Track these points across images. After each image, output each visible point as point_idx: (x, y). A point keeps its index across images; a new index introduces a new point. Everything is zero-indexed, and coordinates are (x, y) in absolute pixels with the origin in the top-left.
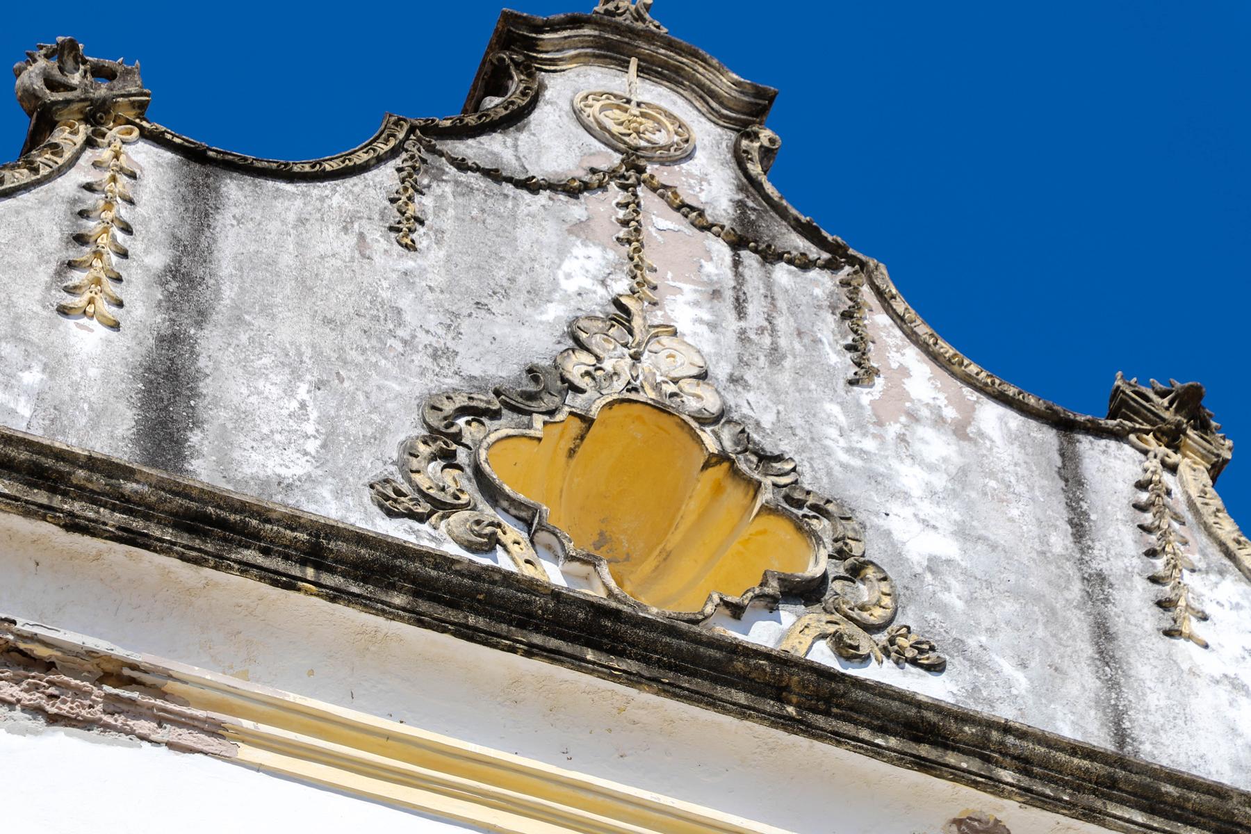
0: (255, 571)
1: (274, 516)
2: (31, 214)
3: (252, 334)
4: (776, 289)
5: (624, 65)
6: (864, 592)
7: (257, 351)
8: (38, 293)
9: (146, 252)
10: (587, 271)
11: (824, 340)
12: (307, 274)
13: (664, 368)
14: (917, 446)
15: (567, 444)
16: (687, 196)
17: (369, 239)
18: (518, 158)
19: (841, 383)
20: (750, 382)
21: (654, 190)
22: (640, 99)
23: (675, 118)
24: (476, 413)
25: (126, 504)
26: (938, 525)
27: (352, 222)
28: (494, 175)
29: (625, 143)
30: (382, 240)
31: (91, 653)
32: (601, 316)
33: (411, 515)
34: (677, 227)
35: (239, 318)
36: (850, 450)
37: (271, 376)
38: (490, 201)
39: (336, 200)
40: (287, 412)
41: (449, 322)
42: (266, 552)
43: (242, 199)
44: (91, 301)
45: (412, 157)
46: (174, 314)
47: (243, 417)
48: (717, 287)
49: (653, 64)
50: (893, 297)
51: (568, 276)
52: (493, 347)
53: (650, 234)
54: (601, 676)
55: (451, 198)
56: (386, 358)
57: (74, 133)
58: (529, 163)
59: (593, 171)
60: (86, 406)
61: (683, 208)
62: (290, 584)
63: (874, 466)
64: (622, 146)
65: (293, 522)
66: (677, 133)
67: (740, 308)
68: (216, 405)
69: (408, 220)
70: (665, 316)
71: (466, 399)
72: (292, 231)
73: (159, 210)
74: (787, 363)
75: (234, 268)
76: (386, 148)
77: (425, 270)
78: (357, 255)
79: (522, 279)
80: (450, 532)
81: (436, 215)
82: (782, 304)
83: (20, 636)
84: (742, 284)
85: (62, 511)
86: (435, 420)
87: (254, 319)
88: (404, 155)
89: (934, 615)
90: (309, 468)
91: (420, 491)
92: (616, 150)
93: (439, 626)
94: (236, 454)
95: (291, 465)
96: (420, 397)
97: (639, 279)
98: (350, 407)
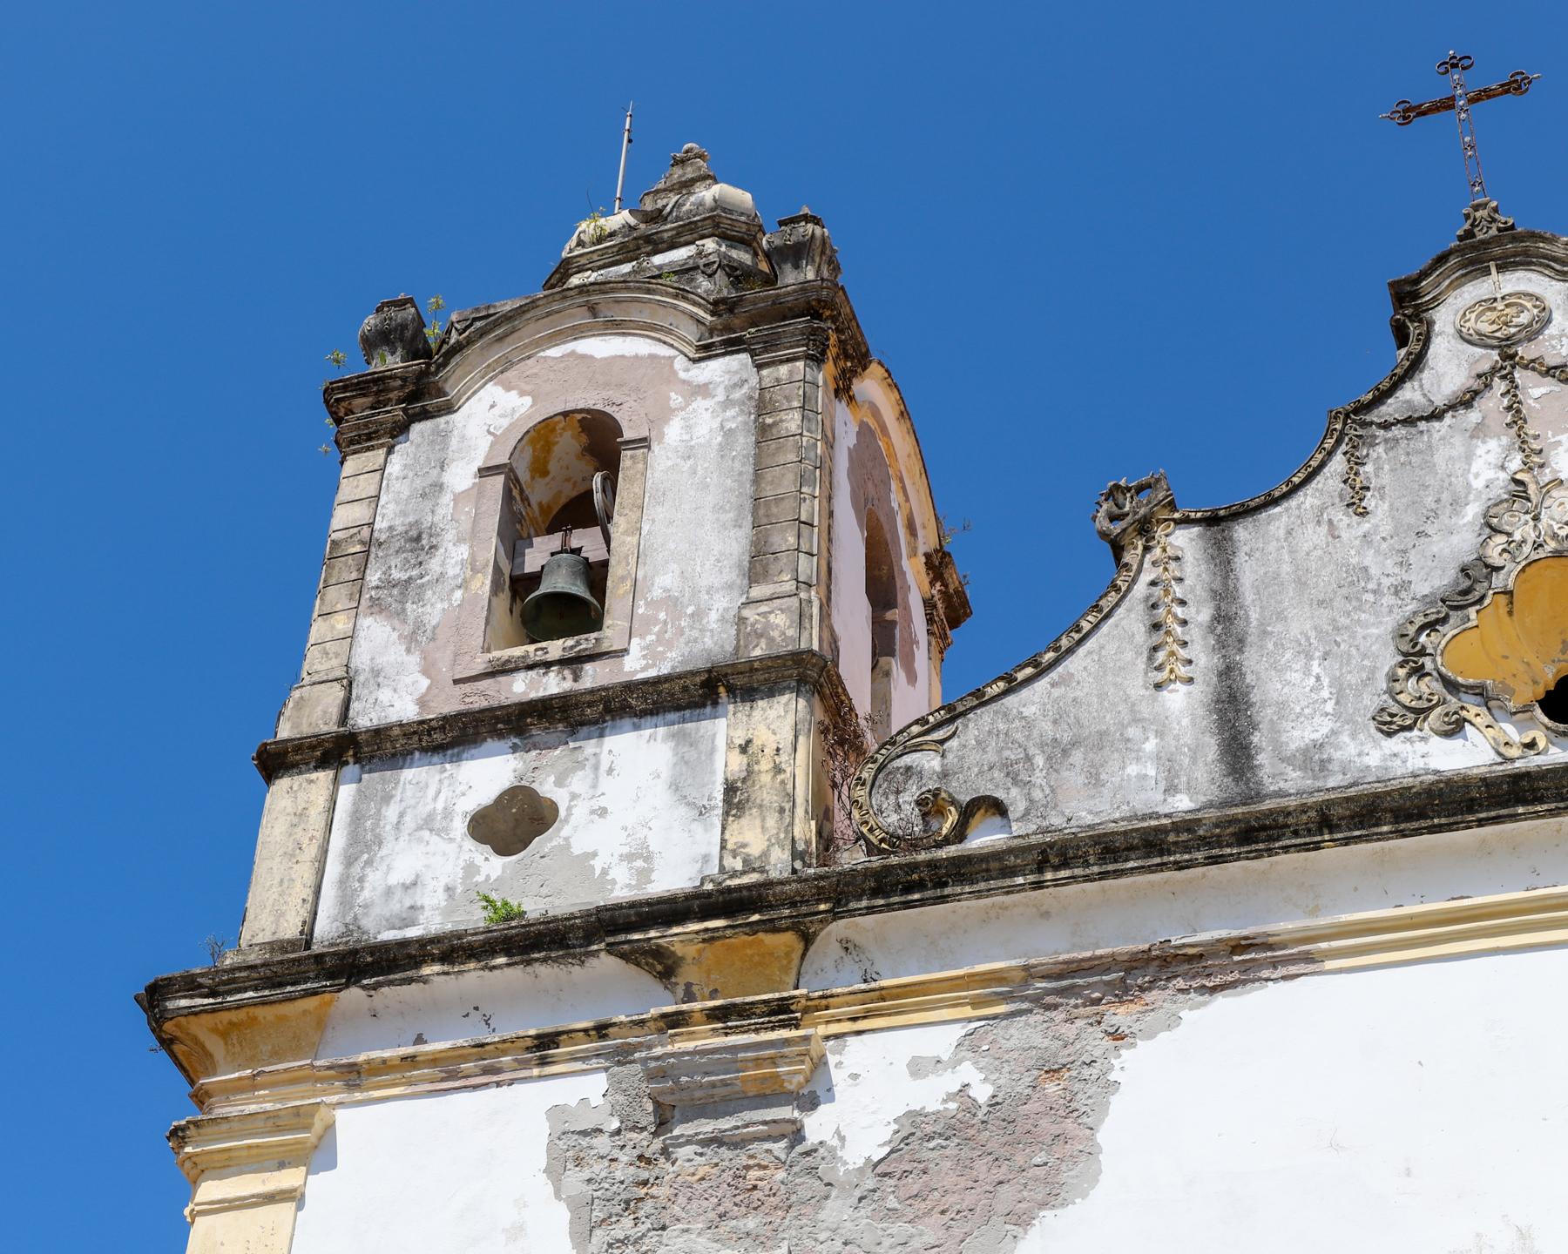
0: (1293, 849)
1: (1291, 809)
2: (1124, 622)
3: (1275, 639)
5: (1486, 272)
7: (1281, 651)
8: (1140, 681)
9: (1198, 612)
10: (1489, 464)
12: (1301, 573)
13: (1557, 518)
15: (1503, 610)
16: (1551, 361)
21: (1526, 367)
22: (1505, 291)
23: (1532, 295)
24: (1431, 626)
25: (1205, 842)
27: (1322, 514)
28: (1409, 421)
29: (1498, 338)
30: (1344, 517)
31: (1218, 941)
32: (1506, 496)
33: (1403, 729)
34: (1549, 389)
35: (1265, 632)
38: (1412, 443)
39: (1309, 501)
40: (1309, 688)
41: (1401, 559)
42: (1296, 834)
43: (1249, 537)
44: (1172, 671)
45: (1351, 439)
46: (1224, 651)
47: (1282, 706)
49: (1508, 257)
51: (1477, 475)
52: (1434, 564)
54: (1532, 819)
55: (1384, 456)
56: (1364, 612)
58: (1434, 395)
59: (1479, 376)
60: (1186, 749)
62: (1317, 847)
64: (1495, 342)
65: (1304, 809)
66: (1535, 307)
68: (1263, 707)
69: (1357, 493)
70: (1554, 471)
71: (1422, 618)
73: (1199, 575)
75: (1255, 594)
76: (1332, 441)
77: (1377, 526)
78: (1330, 539)
79: (1445, 497)
80: (1431, 729)
81: (1377, 476)
83: (1177, 947)
85: (1170, 863)
86: (1406, 647)
88: (1347, 439)
90: (1331, 725)
91: (1405, 707)
92: (1493, 347)
93: (1417, 832)
94: (1284, 739)
95: (1318, 728)
96: (1393, 631)
97: (1528, 450)
98: (1348, 663)
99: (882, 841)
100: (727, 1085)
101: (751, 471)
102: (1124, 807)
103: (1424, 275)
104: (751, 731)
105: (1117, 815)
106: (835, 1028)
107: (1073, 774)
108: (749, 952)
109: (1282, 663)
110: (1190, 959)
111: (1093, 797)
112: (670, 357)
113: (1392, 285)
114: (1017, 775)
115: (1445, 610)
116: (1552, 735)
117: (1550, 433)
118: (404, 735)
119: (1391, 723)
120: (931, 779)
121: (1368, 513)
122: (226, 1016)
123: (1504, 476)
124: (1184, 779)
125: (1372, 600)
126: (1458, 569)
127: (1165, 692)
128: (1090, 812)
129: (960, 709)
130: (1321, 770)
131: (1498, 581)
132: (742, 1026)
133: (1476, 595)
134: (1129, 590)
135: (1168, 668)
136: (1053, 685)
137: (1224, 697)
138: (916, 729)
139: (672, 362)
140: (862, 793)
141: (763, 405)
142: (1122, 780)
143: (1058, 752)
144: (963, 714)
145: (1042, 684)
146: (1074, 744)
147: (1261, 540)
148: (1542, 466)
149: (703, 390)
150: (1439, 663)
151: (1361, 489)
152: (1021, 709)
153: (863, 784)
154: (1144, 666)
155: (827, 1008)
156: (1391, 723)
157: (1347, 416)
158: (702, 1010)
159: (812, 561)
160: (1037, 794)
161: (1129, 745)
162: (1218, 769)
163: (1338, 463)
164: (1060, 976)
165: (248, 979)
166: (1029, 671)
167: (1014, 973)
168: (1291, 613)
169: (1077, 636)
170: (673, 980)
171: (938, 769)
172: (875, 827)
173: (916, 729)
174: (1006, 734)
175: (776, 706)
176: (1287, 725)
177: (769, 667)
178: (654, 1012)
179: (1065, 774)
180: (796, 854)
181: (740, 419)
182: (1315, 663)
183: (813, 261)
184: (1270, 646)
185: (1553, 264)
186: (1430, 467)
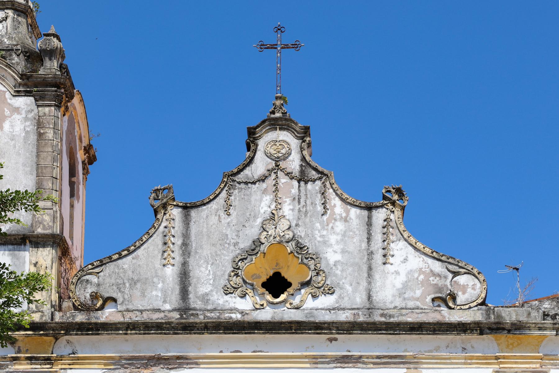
2: (156, 240)
4: (308, 191)
5: (276, 129)
6: (320, 278)
9: (178, 241)
11: (318, 203)
14: (336, 228)
16: (289, 170)
17: (221, 215)
18: (252, 173)
19: (320, 215)
20: (300, 224)
21: (281, 170)
22: (281, 138)
24: (242, 260)
26: (338, 251)
28: (246, 183)
32: (269, 218)
33: (230, 293)
35: (196, 252)
36: (320, 236)
37: (203, 265)
38: (246, 191)
40: (206, 274)
43: (195, 216)
44: (168, 261)
45: (229, 186)
48: (294, 197)
49: (283, 125)
50: (333, 184)
51: (262, 208)
52: (246, 238)
53: (280, 186)
55: (238, 194)
57: (161, 213)
59: (268, 170)
60: (170, 289)
61: (287, 174)
63: (325, 239)
66: (288, 147)
67: (299, 202)
71: (240, 257)
72: (205, 221)
74: (308, 215)
76: (223, 185)
78: (219, 222)
79: (252, 213)
81: (234, 201)
82: (308, 196)
84: (300, 193)
86: (234, 266)
87: (199, 251)
89: (334, 278)
90: (211, 288)
92: (273, 160)
94: (198, 290)
96: (232, 259)
97: (277, 202)
98: (218, 268)
99: (79, 305)
101: (36, 152)
102: (151, 305)
103: (258, 127)
104: (37, 259)
105: (149, 308)
106: (64, 366)
107: (137, 291)
108: (39, 340)
109: (200, 264)
110: (165, 359)
111: (142, 300)
112: (4, 91)
113: (248, 128)
114: (121, 289)
115: (246, 255)
116: (268, 303)
117: (284, 197)
119: (227, 290)
120: (94, 285)
121: (230, 215)
123: (269, 210)
124: (169, 299)
125: (228, 247)
126: (252, 241)
127: (166, 268)
128: (141, 305)
129: (104, 262)
130: (207, 303)
131: (262, 247)
132: (36, 363)
133: (256, 251)
134: (158, 228)
135: (168, 260)
136: (133, 258)
137: (183, 272)
138: (90, 267)
139: (5, 94)
140: (73, 287)
141: (39, 124)
142: (151, 296)
143: (133, 283)
144: (105, 264)
145: (130, 258)
146: (138, 281)
147: (199, 218)
148: (280, 209)
149: (17, 110)
150: (243, 274)
151: (229, 205)
152: (123, 266)
153: (73, 284)
154: (160, 257)
155: (62, 360)
156: (227, 290)
157: (229, 176)
158: (24, 357)
159: (57, 194)
160: (126, 297)
161: (154, 284)
162: (179, 297)
163: (224, 194)
164: (129, 359)
166: (126, 252)
167: (117, 357)
168: (205, 246)
169: (141, 243)
170: (15, 345)
171: (97, 282)
172: (77, 300)
173: (90, 267)
174: (118, 274)
175: (46, 251)
176: (199, 286)
177: (44, 237)
178: (9, 356)
179: (135, 291)
180: (52, 306)
181: (31, 127)
182: (209, 266)
183: (57, 57)
184: (197, 257)
185: (295, 132)
186: (249, 201)
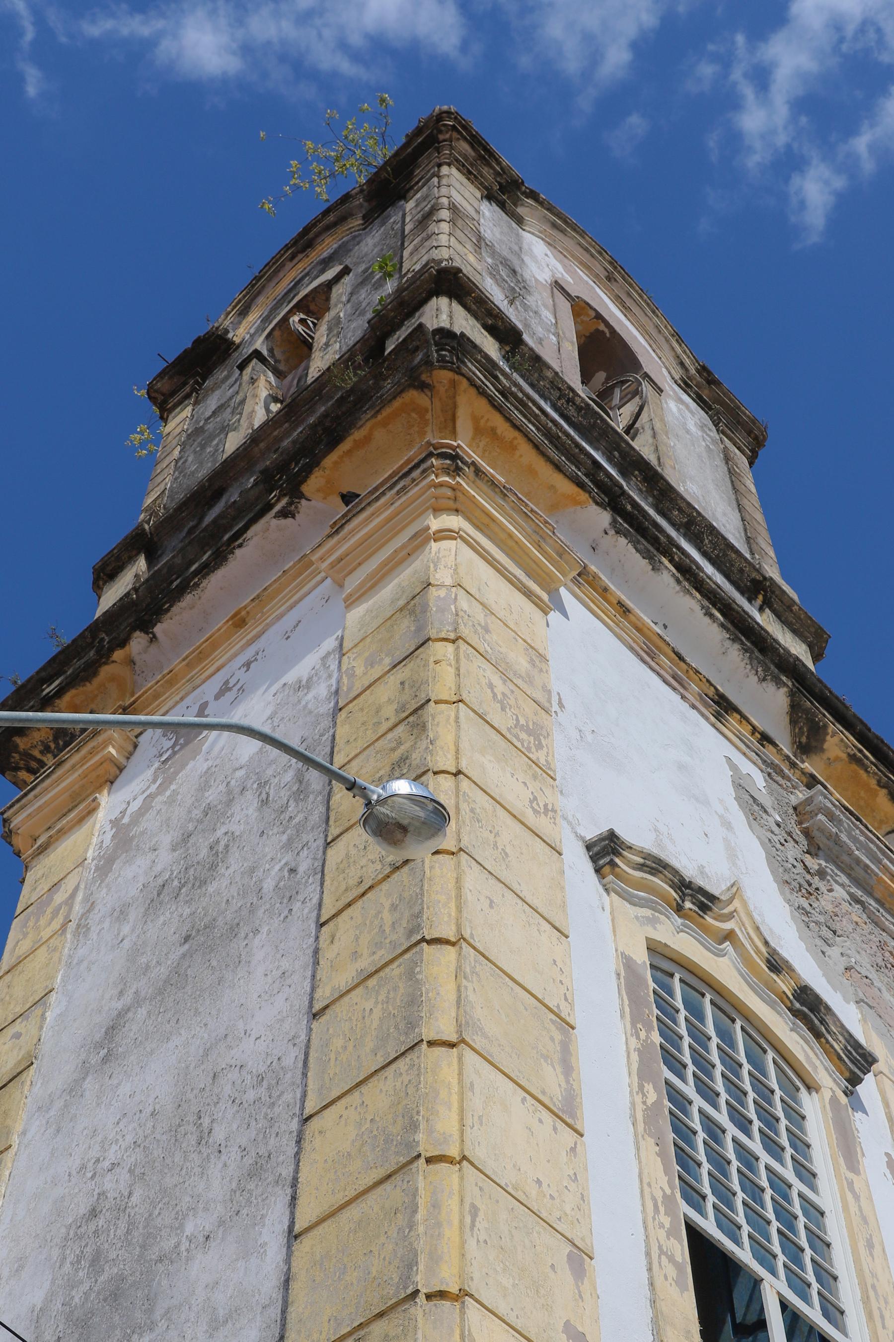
100: (866, 872)
108: (862, 794)
118: (552, 382)
122: (497, 421)
165: (536, 416)
170: (804, 757)
177: (801, 620)
